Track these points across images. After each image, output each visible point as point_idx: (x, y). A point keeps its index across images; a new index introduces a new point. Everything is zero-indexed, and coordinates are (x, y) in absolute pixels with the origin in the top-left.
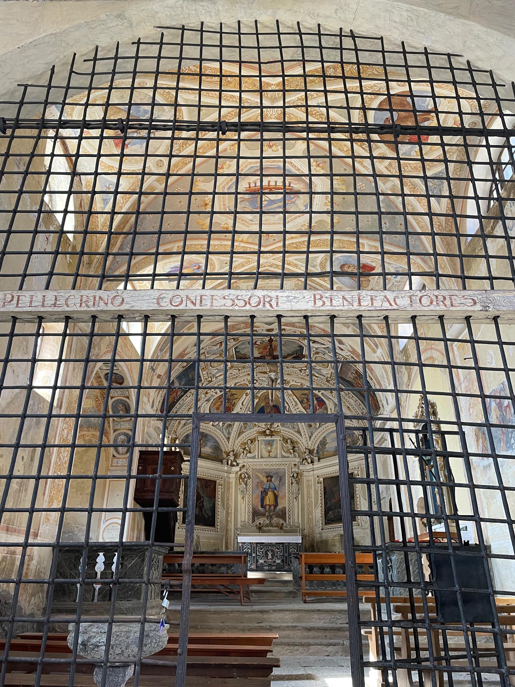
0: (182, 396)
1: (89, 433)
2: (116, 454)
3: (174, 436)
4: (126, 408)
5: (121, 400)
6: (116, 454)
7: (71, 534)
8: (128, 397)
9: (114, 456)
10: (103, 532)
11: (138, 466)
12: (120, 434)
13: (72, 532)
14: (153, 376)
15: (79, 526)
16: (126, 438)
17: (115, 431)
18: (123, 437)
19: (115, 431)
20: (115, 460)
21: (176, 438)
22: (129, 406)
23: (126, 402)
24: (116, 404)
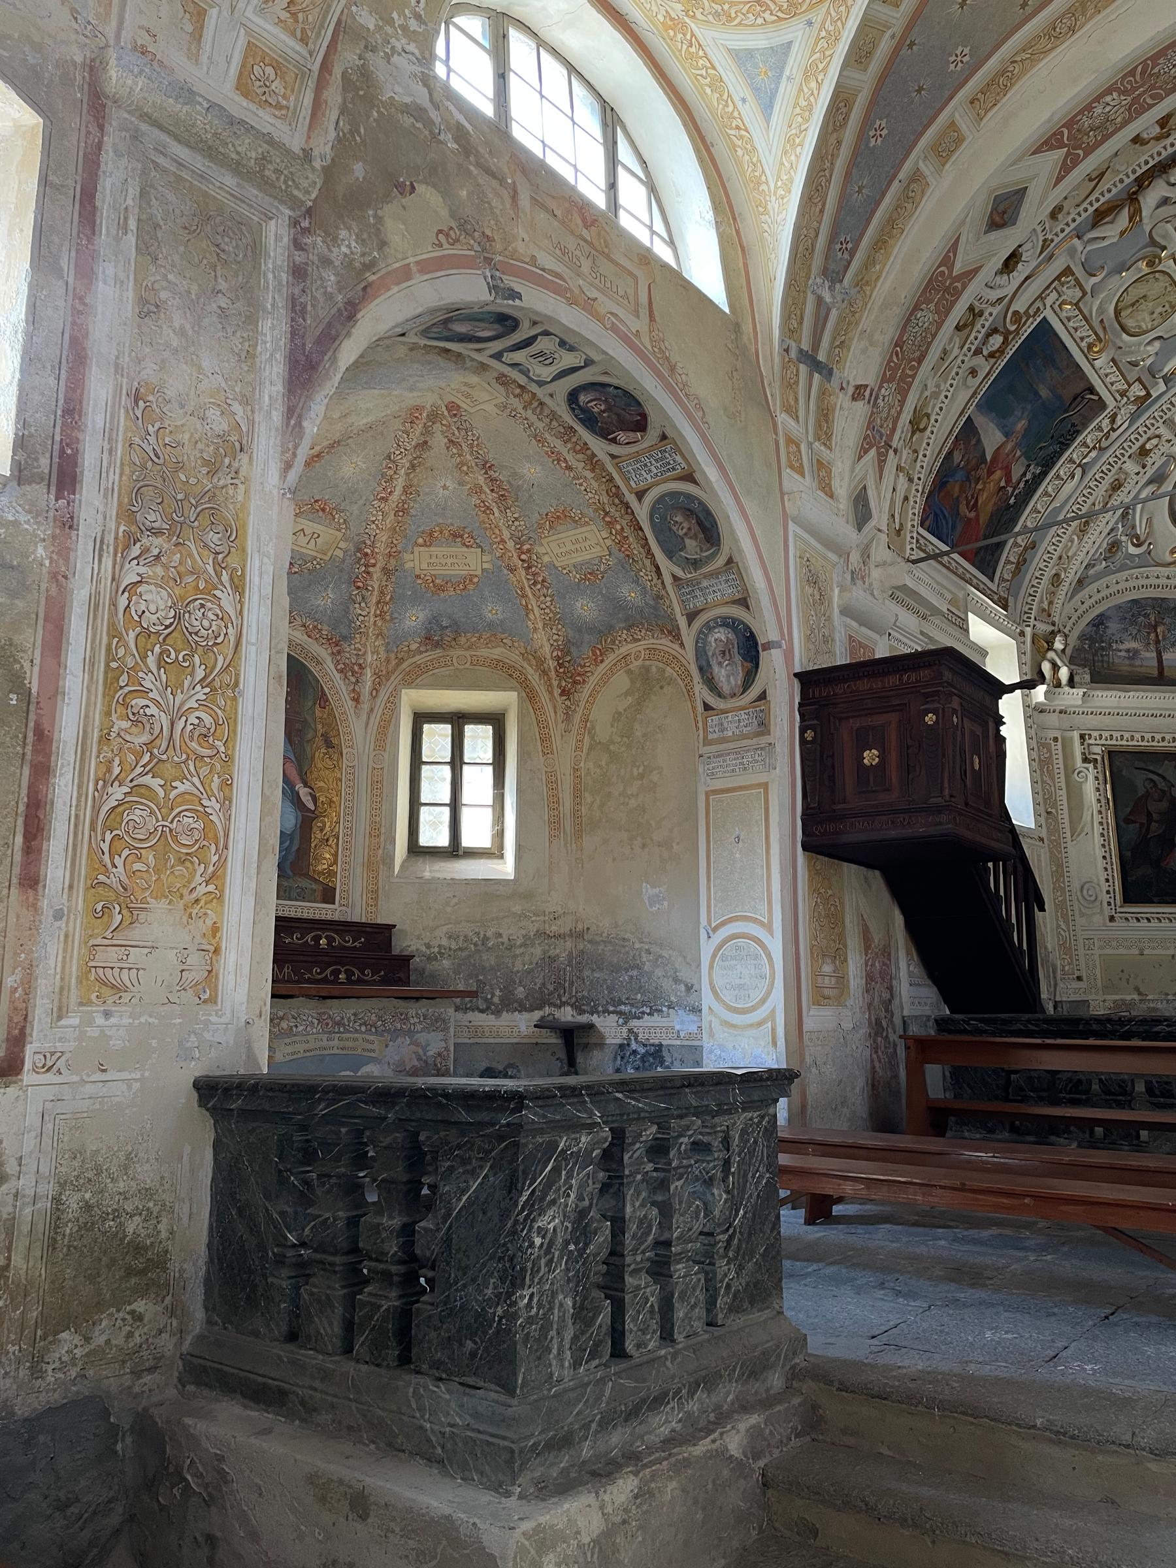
0: (1038, 480)
1: (640, 646)
2: (712, 701)
3: (1043, 628)
4: (700, 523)
5: (673, 494)
6: (712, 701)
7: (635, 973)
8: (689, 477)
9: (707, 707)
10: (711, 967)
11: (802, 731)
12: (709, 627)
13: (638, 967)
14: (823, 393)
15: (653, 949)
16: (731, 636)
17: (691, 617)
18: (721, 634)
19: (691, 617)
20: (713, 721)
21: (1053, 634)
22: (708, 513)
23: (689, 497)
24: (663, 518)
